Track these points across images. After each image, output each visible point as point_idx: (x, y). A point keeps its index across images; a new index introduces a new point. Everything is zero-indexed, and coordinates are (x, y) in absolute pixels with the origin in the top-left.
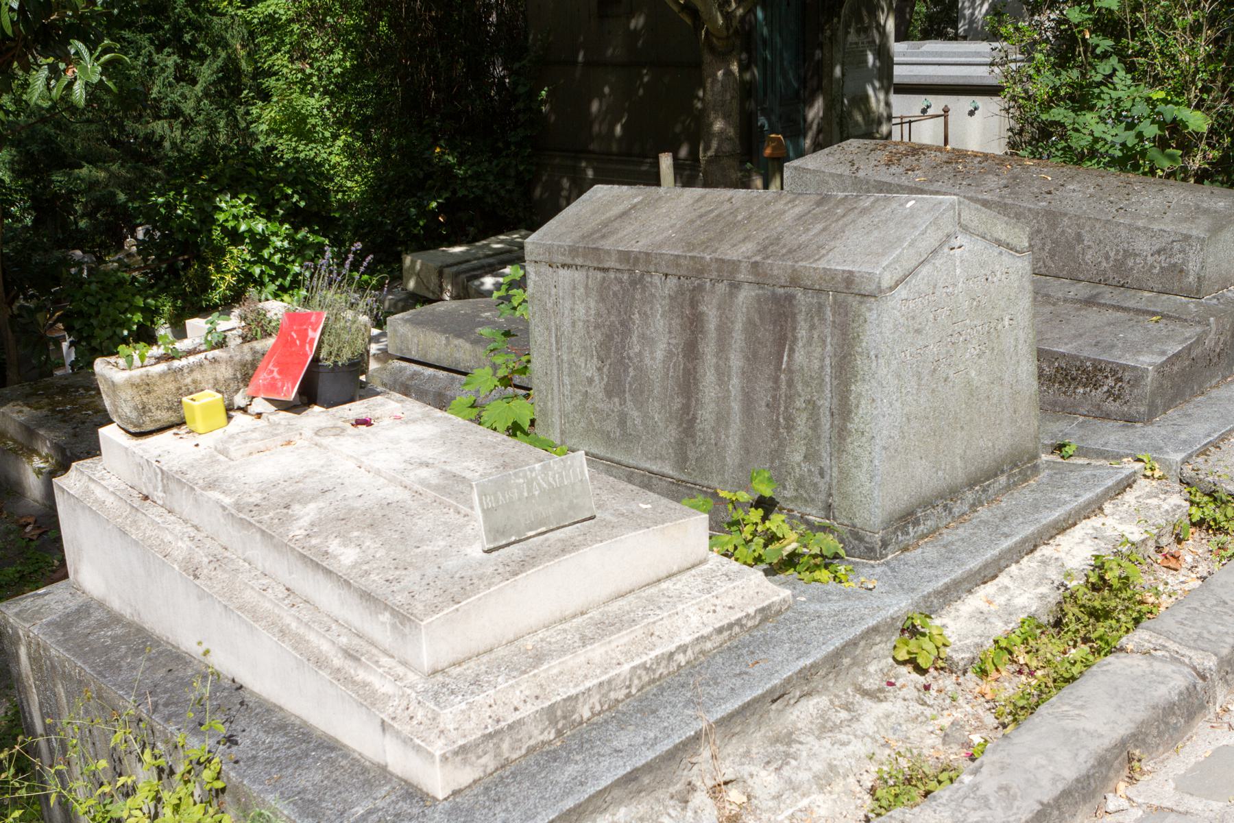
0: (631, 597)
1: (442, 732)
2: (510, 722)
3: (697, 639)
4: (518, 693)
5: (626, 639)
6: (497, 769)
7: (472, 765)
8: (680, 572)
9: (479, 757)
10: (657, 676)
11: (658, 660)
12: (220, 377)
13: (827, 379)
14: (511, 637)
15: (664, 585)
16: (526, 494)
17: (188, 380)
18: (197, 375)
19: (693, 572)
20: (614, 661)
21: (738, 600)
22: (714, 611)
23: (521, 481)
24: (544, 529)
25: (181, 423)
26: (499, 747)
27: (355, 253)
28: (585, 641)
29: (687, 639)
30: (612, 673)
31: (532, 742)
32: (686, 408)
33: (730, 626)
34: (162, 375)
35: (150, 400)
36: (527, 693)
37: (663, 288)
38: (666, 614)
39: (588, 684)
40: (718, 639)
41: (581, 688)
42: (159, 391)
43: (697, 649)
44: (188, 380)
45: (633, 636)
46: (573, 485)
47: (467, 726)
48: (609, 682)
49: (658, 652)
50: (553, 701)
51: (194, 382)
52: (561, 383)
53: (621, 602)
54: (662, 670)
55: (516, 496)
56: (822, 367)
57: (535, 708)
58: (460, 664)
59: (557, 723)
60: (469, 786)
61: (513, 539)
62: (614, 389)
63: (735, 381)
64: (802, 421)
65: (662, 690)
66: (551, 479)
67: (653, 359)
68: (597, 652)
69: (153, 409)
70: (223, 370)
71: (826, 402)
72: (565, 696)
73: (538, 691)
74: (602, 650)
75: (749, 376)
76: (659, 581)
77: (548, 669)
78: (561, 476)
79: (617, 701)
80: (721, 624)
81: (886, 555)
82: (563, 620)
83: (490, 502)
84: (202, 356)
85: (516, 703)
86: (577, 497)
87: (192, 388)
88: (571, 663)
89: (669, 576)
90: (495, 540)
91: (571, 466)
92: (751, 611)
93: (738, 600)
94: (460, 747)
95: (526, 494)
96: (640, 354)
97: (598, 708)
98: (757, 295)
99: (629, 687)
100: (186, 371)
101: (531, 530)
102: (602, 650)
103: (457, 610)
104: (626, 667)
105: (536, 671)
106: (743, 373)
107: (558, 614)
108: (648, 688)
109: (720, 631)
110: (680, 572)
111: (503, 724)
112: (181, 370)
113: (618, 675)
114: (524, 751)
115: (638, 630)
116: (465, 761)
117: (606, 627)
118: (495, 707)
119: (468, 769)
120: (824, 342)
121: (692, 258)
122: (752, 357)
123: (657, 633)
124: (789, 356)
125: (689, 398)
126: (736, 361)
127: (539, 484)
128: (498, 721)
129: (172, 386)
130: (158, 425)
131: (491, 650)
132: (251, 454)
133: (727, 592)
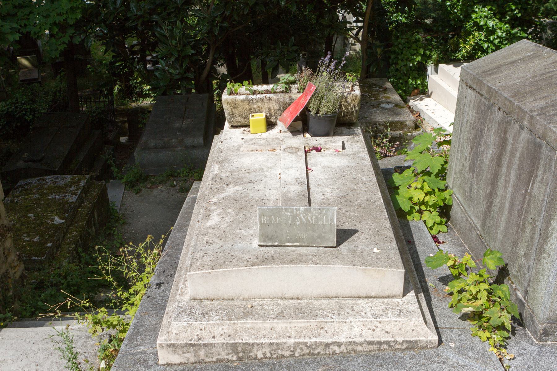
0: (333, 301)
1: (169, 332)
2: (205, 342)
3: (350, 342)
4: (220, 329)
5: (303, 325)
6: (196, 362)
7: (180, 355)
8: (376, 297)
9: (184, 353)
10: (316, 352)
11: (317, 345)
12: (272, 107)
13: (543, 210)
14: (246, 296)
15: (360, 301)
16: (290, 222)
17: (256, 106)
18: (260, 104)
19: (386, 300)
20: (288, 334)
21: (396, 330)
22: (374, 330)
23: (289, 214)
24: (298, 244)
25: (248, 126)
26: (197, 352)
27: (347, 59)
28: (281, 315)
29: (342, 340)
30: (281, 340)
31: (220, 357)
32: (491, 193)
33: (380, 343)
34: (243, 101)
35: (236, 112)
36: (226, 331)
37: (498, 116)
38: (337, 320)
39: (262, 341)
40: (369, 348)
41: (257, 341)
42: (241, 108)
43: (350, 347)
44: (256, 106)
45: (309, 324)
46: (324, 225)
47: (183, 335)
48: (278, 344)
49: (318, 340)
50: (236, 341)
51: (258, 107)
52: (458, 155)
53: (325, 301)
54: (320, 350)
55: (284, 221)
56: (543, 200)
57: (223, 341)
58: (212, 300)
59: (238, 353)
60: (178, 364)
61: (276, 244)
62: (472, 169)
63: (510, 189)
64: (528, 229)
65: (313, 361)
66: (309, 218)
67: (486, 157)
68: (280, 325)
69: (237, 116)
70: (274, 104)
71: (539, 224)
72: (244, 342)
73: (232, 332)
74: (284, 325)
75: (515, 191)
76: (359, 297)
77: (244, 323)
78: (317, 217)
79: (283, 356)
80: (373, 340)
81: (546, 341)
82: (283, 298)
83: (266, 220)
84: (264, 95)
85: (216, 334)
86: (325, 233)
87: (257, 110)
88: (260, 325)
89: (367, 297)
90: (265, 241)
91: (325, 214)
92: (400, 339)
93: (396, 330)
94: (171, 344)
95: (290, 222)
96: (483, 151)
97: (268, 355)
98: (529, 138)
99: (293, 351)
100: (254, 101)
101: (289, 242)
102: (284, 325)
103: (210, 273)
104: (292, 341)
105: (236, 322)
106: (514, 186)
107: (280, 295)
108: (308, 357)
109: (371, 343)
110: (376, 297)
111: (200, 342)
112: (252, 100)
113: (285, 343)
114: (214, 359)
115: (313, 323)
116: (175, 352)
117: (300, 312)
118: (203, 331)
119: (177, 356)
120: (548, 184)
121: (511, 102)
122: (518, 178)
123: (326, 329)
124: (532, 186)
125: (493, 190)
126: (513, 178)
127: (301, 219)
128: (199, 339)
129: (247, 107)
130: (239, 124)
131: (232, 299)
132: (252, 151)
133: (389, 322)
